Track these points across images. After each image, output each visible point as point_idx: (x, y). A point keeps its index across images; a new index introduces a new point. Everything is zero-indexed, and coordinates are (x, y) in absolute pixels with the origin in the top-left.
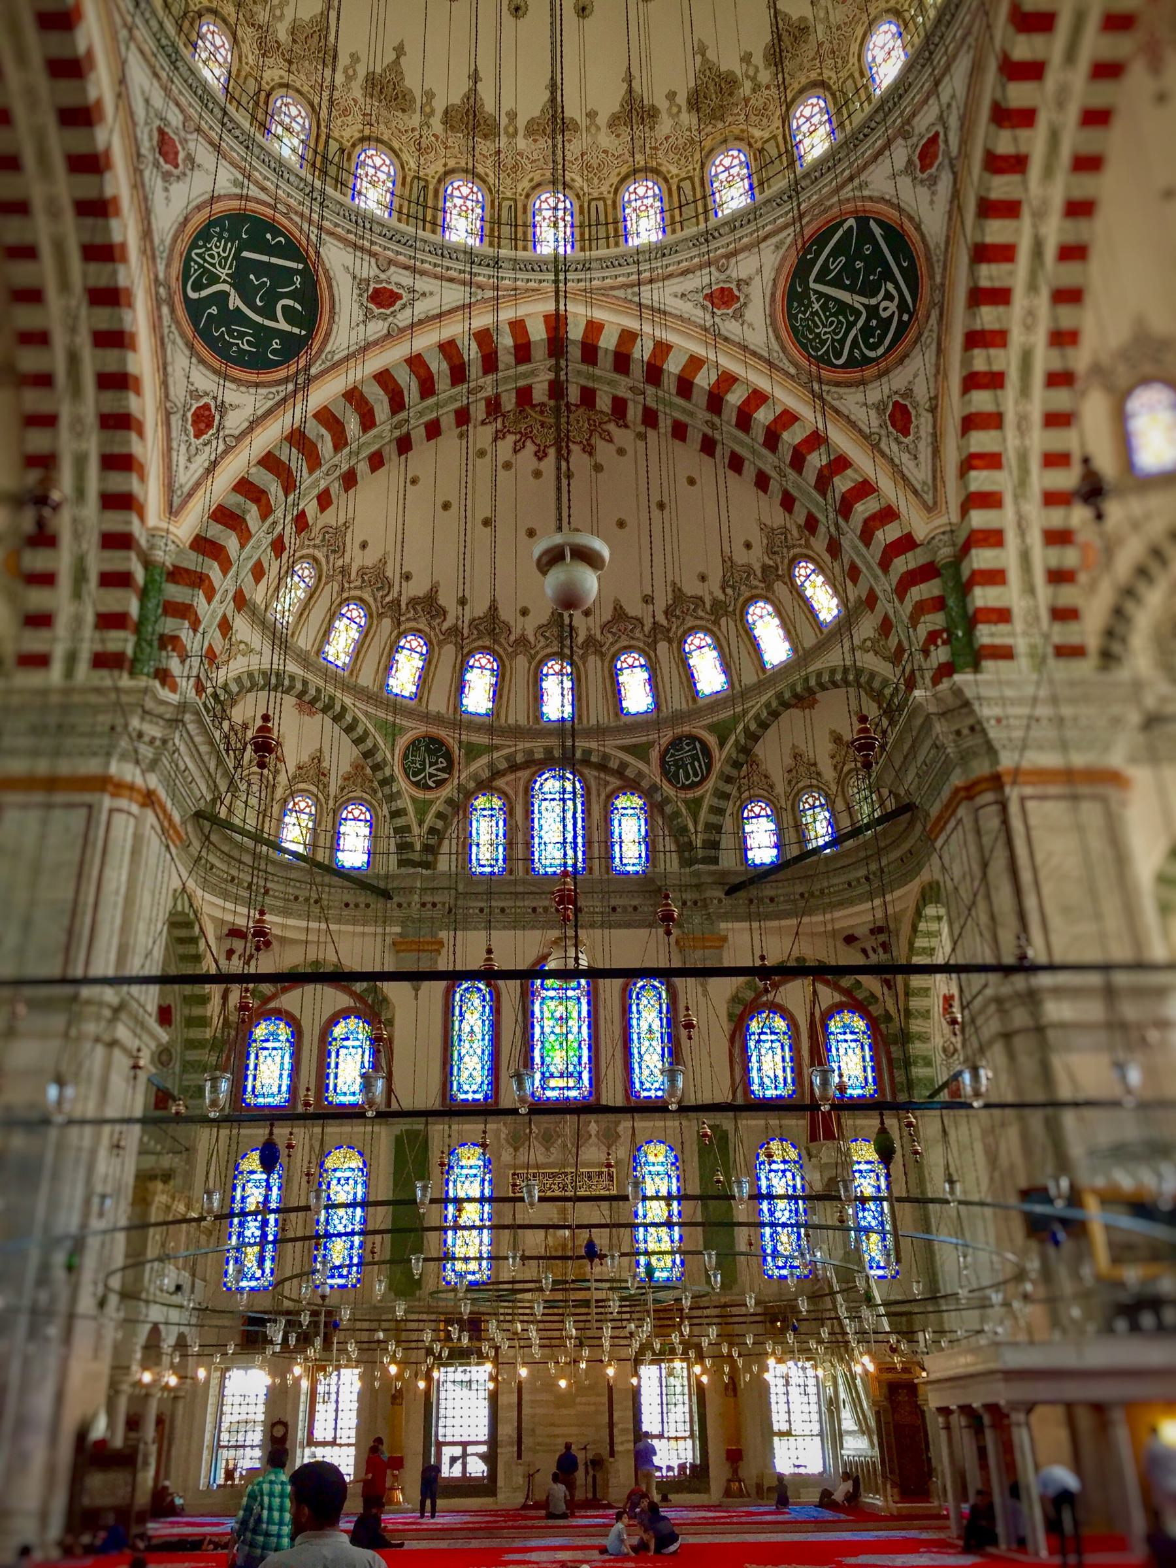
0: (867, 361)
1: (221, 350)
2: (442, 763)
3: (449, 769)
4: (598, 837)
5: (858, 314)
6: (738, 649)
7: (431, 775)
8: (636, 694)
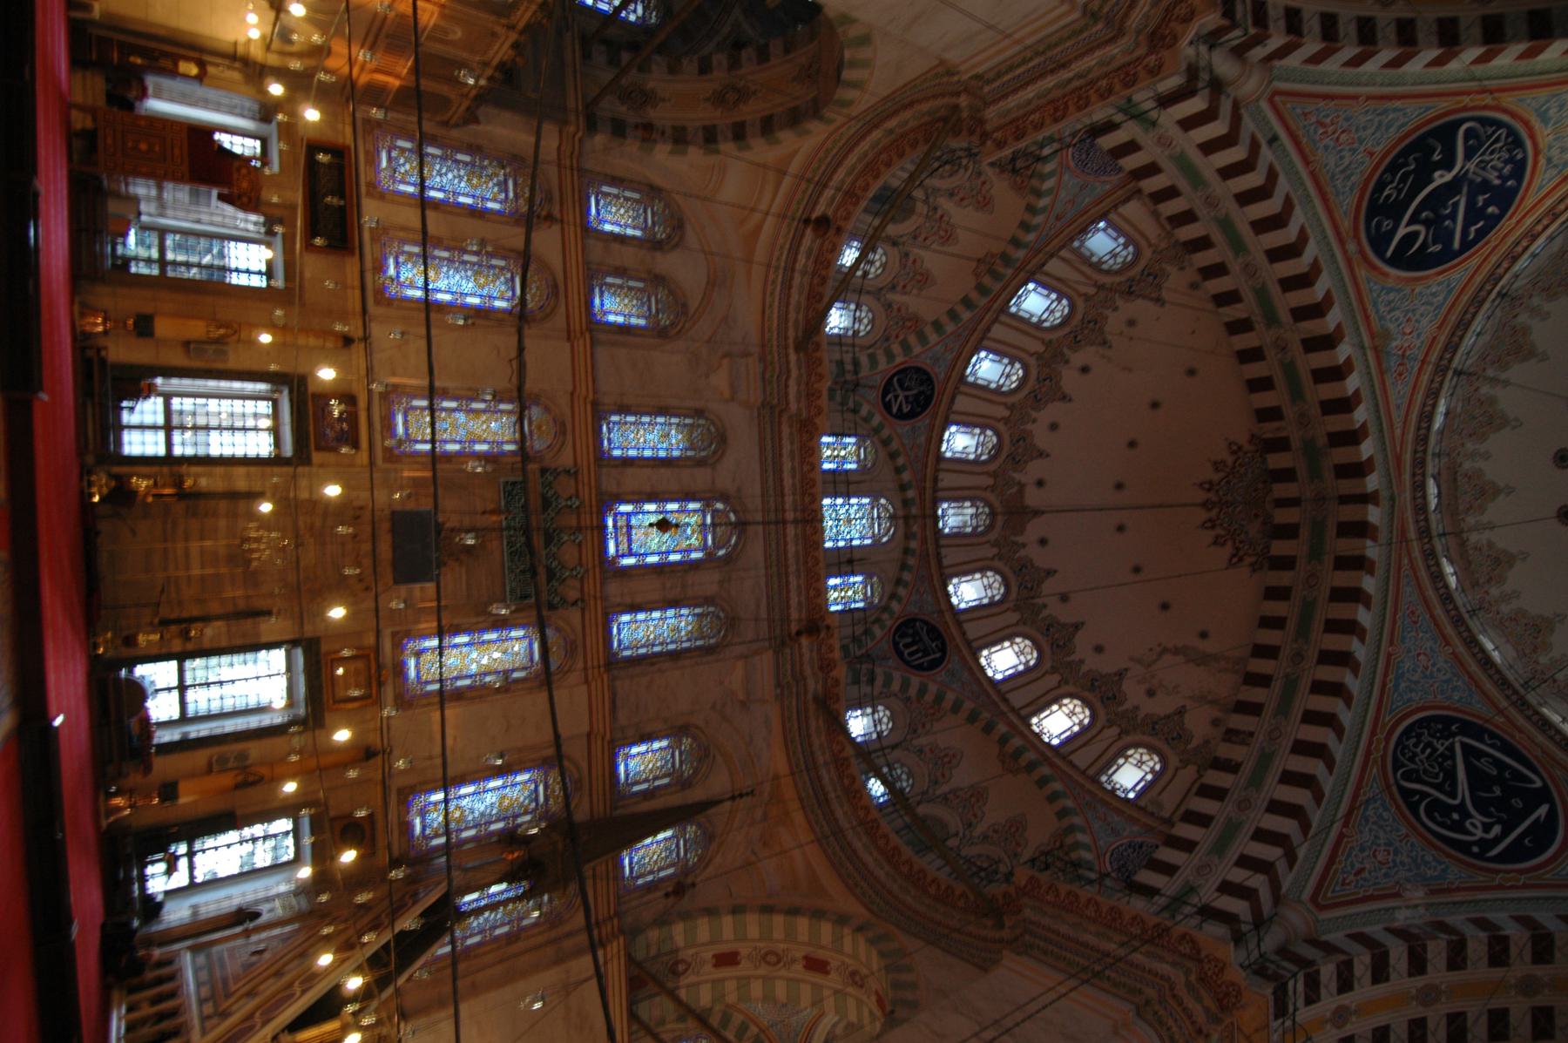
0: (1414, 808)
2: (906, 409)
3: (901, 416)
4: (848, 561)
5: (1455, 798)
6: (1036, 689)
7: (896, 397)
8: (967, 592)
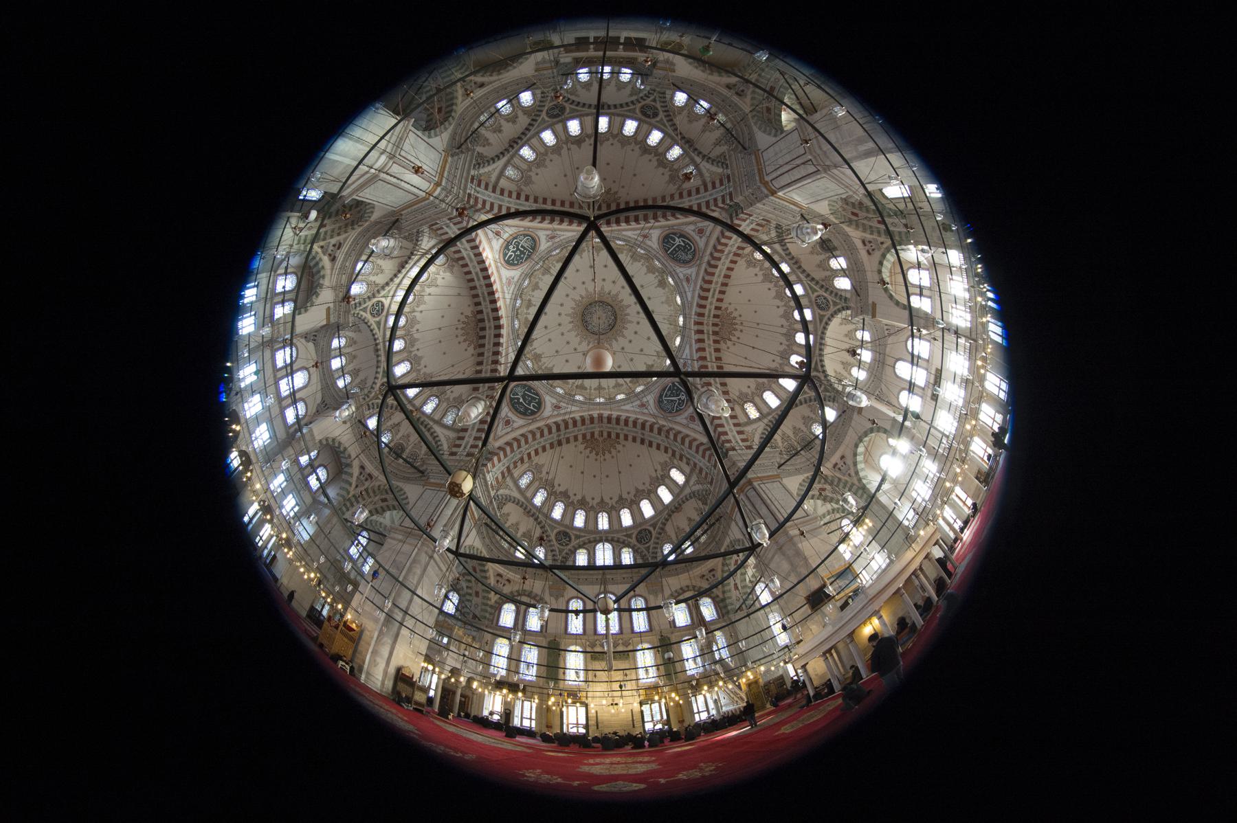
1: (516, 410)
